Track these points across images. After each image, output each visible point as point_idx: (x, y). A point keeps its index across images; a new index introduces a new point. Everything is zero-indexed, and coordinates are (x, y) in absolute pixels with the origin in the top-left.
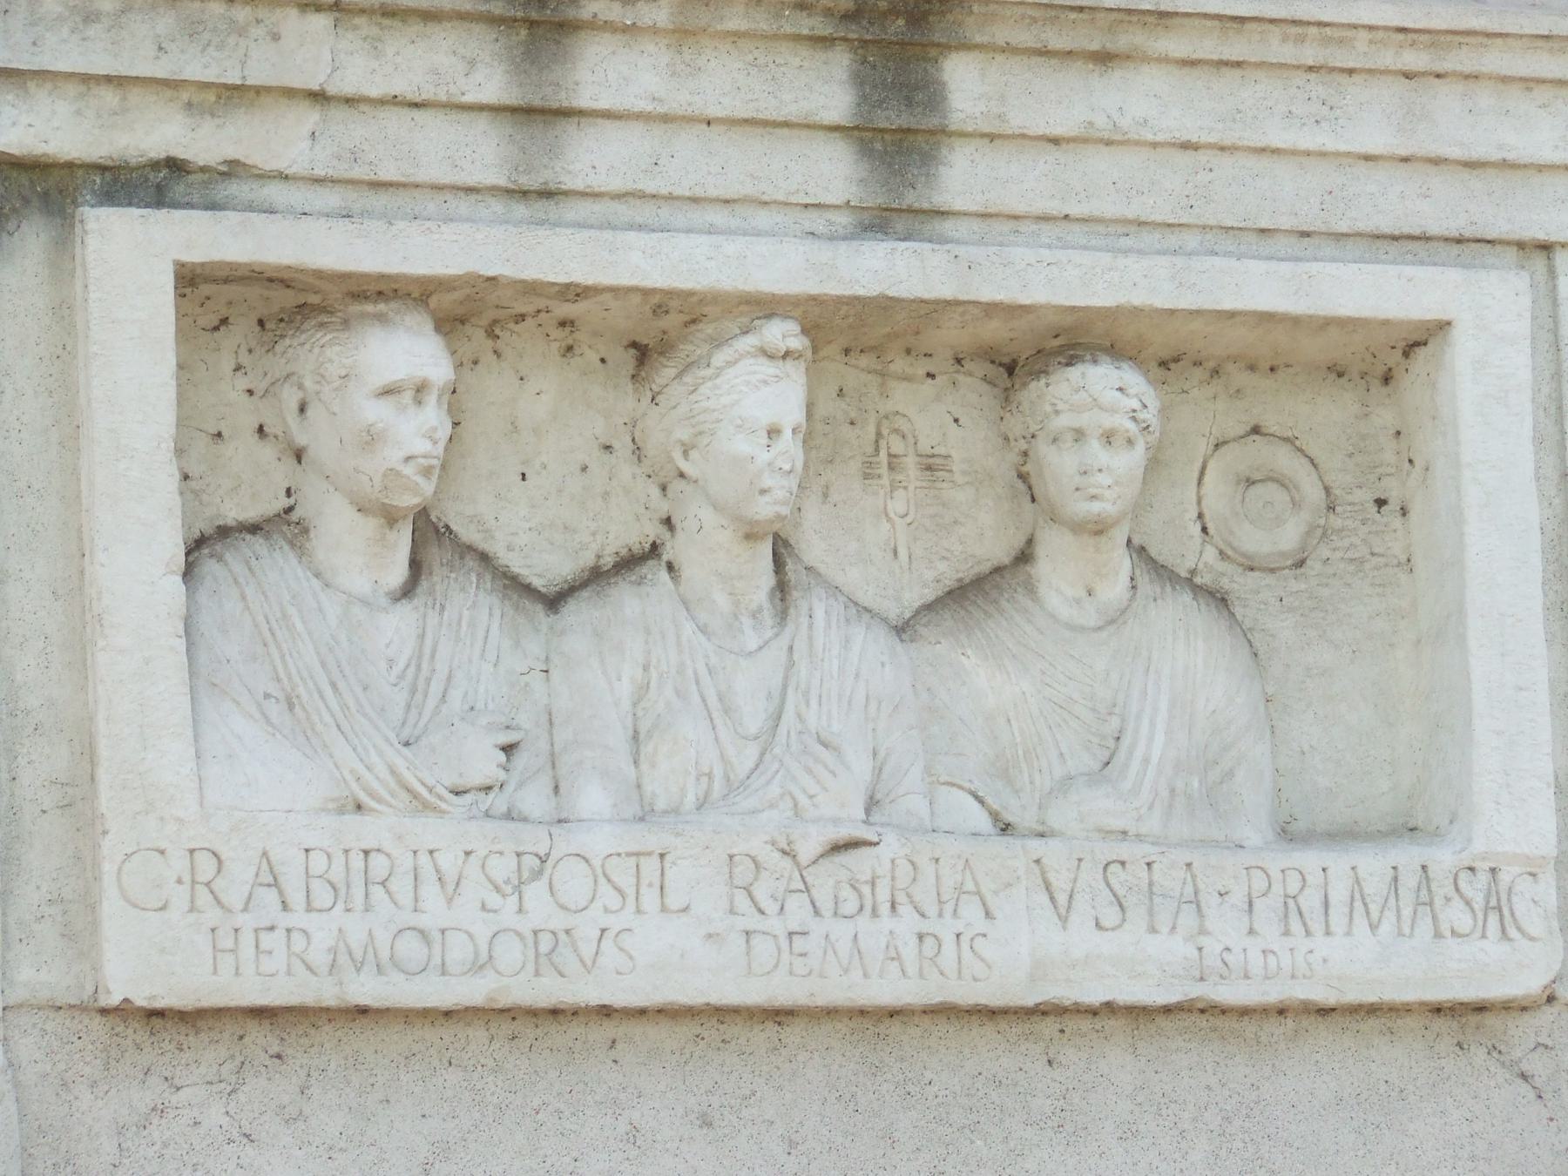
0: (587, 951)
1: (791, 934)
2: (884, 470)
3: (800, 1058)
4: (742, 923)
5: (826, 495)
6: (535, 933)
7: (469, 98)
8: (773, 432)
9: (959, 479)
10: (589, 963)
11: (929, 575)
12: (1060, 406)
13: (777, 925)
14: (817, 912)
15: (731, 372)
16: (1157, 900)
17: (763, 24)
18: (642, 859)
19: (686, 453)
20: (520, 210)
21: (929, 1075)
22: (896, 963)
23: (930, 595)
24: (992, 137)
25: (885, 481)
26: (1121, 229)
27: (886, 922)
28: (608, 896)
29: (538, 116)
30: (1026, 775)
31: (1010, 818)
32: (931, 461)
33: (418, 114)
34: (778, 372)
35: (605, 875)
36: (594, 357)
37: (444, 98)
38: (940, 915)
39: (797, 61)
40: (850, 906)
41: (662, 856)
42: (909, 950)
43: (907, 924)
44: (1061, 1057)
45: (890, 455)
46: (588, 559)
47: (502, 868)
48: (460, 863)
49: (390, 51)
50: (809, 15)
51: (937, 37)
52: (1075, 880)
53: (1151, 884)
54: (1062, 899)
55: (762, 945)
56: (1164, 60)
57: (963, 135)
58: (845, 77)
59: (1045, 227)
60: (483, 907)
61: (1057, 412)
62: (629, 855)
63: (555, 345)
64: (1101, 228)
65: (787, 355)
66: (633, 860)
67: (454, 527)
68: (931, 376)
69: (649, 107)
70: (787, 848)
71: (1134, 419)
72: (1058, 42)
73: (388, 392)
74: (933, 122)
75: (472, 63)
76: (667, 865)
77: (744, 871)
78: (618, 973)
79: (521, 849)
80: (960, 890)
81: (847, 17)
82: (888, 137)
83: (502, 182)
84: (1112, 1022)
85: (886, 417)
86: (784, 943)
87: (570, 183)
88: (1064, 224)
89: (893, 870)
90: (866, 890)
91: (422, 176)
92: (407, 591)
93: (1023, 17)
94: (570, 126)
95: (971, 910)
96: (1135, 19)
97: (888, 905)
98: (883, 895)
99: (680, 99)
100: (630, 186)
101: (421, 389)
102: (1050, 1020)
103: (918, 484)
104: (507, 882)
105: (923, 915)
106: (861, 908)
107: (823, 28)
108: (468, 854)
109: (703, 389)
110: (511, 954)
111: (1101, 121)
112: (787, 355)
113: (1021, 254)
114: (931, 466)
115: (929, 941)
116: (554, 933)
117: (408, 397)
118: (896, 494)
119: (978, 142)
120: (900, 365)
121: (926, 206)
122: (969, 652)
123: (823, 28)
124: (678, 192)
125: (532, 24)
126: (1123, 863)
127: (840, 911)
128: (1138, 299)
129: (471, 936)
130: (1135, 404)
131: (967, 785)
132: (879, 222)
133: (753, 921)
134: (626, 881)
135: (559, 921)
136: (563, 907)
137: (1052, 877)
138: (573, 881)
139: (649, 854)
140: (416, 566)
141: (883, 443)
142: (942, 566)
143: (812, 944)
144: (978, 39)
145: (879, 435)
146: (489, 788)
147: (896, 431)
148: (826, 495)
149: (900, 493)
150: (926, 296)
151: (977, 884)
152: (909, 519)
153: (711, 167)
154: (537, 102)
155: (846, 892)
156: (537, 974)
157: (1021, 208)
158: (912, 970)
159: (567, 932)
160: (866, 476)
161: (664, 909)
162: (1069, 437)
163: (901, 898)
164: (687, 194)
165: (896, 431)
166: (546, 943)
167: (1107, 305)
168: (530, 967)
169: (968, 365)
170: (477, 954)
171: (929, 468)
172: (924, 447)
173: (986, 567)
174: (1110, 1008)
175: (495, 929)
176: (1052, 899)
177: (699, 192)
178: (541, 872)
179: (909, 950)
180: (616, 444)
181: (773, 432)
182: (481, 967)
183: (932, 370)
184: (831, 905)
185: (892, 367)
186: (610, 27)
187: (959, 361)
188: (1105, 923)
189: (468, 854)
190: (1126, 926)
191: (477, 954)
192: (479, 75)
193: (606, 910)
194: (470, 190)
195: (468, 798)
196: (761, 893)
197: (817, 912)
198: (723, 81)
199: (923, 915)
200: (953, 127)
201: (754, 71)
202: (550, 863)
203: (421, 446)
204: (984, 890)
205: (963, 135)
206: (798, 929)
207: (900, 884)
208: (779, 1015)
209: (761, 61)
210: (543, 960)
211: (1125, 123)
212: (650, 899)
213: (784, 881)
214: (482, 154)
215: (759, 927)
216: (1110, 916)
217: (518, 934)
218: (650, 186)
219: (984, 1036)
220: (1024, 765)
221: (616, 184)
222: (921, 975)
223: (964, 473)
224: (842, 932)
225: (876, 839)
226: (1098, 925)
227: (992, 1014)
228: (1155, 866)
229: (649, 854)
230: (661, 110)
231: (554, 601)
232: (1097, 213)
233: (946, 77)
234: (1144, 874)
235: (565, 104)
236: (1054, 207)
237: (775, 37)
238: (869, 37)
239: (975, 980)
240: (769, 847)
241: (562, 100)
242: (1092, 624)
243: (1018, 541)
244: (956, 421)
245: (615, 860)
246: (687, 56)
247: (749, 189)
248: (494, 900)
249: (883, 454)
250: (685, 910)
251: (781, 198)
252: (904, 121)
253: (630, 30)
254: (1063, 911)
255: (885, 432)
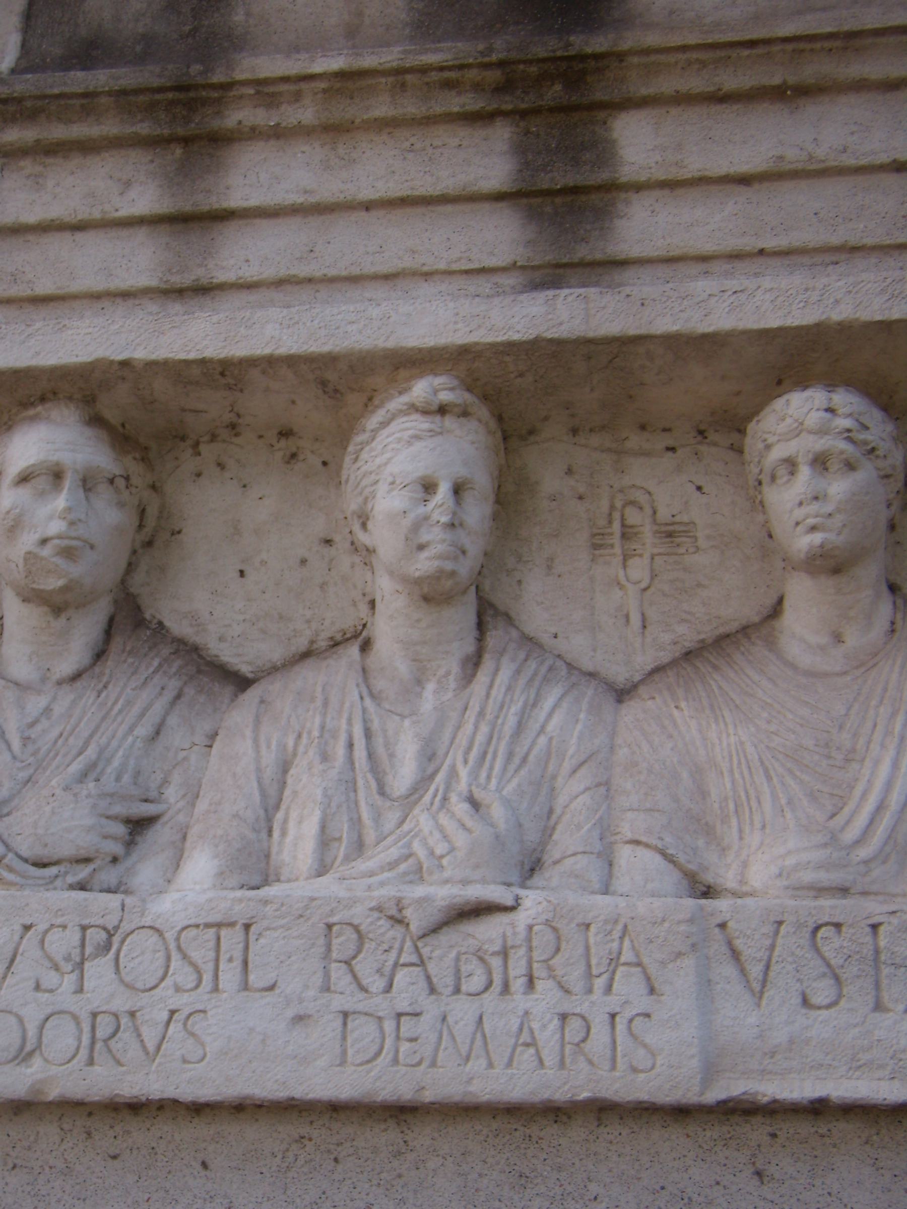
0: (150, 1037)
1: (399, 1015)
2: (616, 540)
3: (431, 1165)
4: (338, 1002)
5: (549, 568)
6: (94, 1015)
7: (123, 213)
8: (429, 487)
9: (701, 543)
10: (151, 1047)
11: (666, 638)
12: (771, 439)
13: (382, 1005)
14: (432, 990)
15: (385, 432)
16: (885, 971)
17: (411, 107)
18: (223, 932)
19: (364, 526)
20: (176, 307)
21: (594, 1188)
22: (532, 1051)
23: (665, 657)
24: (670, 185)
25: (618, 550)
26: (828, 258)
27: (520, 1001)
28: (181, 973)
29: (193, 222)
30: (735, 830)
31: (709, 878)
32: (671, 528)
33: (79, 236)
34: (432, 426)
35: (179, 948)
36: (316, 461)
37: (97, 215)
38: (590, 991)
39: (456, 142)
40: (476, 982)
41: (247, 927)
42: (547, 1035)
43: (545, 1000)
44: (772, 1169)
45: (623, 525)
46: (301, 644)
47: (63, 943)
48: (16, 937)
49: (50, 184)
50: (459, 94)
51: (599, 96)
52: (772, 947)
53: (877, 952)
54: (755, 971)
55: (363, 1032)
56: (860, 86)
57: (638, 187)
58: (505, 148)
59: (738, 264)
60: (38, 988)
61: (768, 447)
62: (208, 926)
63: (281, 453)
64: (806, 260)
65: (442, 410)
66: (212, 931)
67: (167, 623)
68: (672, 449)
69: (300, 199)
70: (398, 916)
71: (850, 440)
72: (730, 81)
73: (24, 479)
74: (603, 176)
75: (128, 184)
76: (252, 937)
77: (344, 942)
78: (185, 1061)
79: (86, 922)
80: (614, 961)
81: (499, 90)
82: (558, 200)
83: (154, 283)
84: (842, 1125)
85: (621, 491)
86: (389, 1026)
87: (221, 277)
88: (761, 260)
89: (529, 939)
90: (496, 963)
91: (76, 287)
92: (76, 677)
93: (689, 63)
94: (231, 229)
95: (628, 985)
96: (818, 45)
97: (523, 980)
98: (518, 968)
99: (331, 188)
100: (283, 273)
101: (57, 475)
102: (757, 1120)
103: (656, 551)
104: (68, 958)
105: (567, 992)
106: (489, 985)
107: (470, 102)
108: (27, 928)
109: (364, 455)
110: (62, 1039)
111: (791, 154)
112: (442, 410)
113: (703, 286)
114: (670, 533)
115: (575, 1024)
116: (116, 1016)
117: (42, 482)
118: (630, 562)
119: (657, 193)
120: (635, 440)
121: (598, 256)
122: (683, 704)
123: (470, 102)
124: (332, 272)
125: (186, 141)
126: (838, 926)
127: (464, 988)
128: (838, 314)
129: (21, 1021)
130: (847, 423)
131: (654, 841)
132: (549, 275)
133: (349, 1000)
134: (202, 954)
135: (122, 1003)
136: (129, 986)
137: (739, 943)
138: (141, 956)
139: (232, 924)
140: (99, 655)
141: (617, 516)
142: (681, 629)
143: (425, 1026)
144: (644, 91)
145: (612, 507)
146: (87, 860)
147: (632, 503)
148: (549, 568)
149: (632, 562)
150: (591, 334)
151: (637, 955)
152: (643, 585)
153: (373, 254)
154: (188, 208)
155: (471, 966)
156: (91, 1062)
157: (709, 247)
158: (550, 1059)
159: (132, 1014)
160: (596, 547)
161: (245, 986)
162: (782, 471)
163: (539, 970)
164: (344, 273)
165: (632, 503)
166: (104, 1027)
167: (804, 323)
168: (84, 1053)
169: (712, 436)
170: (24, 1039)
171: (670, 535)
172: (664, 514)
173: (734, 626)
174: (818, 1109)
175: (49, 1010)
176: (743, 971)
177: (355, 271)
178: (108, 946)
179: (547, 1035)
180: (337, 538)
181: (429, 487)
182: (31, 1054)
183: (671, 443)
184: (450, 980)
185: (628, 445)
186: (254, 134)
187: (701, 432)
188: (816, 1000)
189: (27, 928)
190: (843, 1003)
191: (24, 1039)
192: (133, 194)
193: (178, 989)
194: (126, 295)
195: (53, 870)
196: (365, 967)
197: (432, 990)
198: (379, 168)
199: (567, 992)
200: (623, 180)
201: (410, 156)
202: (116, 940)
203: (56, 527)
204: (646, 960)
205: (638, 187)
206: (408, 1009)
207: (536, 955)
208: (401, 1113)
209: (418, 146)
210: (99, 1045)
211: (820, 152)
212: (229, 976)
213: (393, 955)
214: (138, 261)
215: (360, 1007)
216: (822, 992)
217: (75, 1018)
218: (303, 270)
219: (669, 1141)
220: (734, 822)
221: (269, 273)
222: (562, 1064)
223: (709, 537)
224: (463, 1012)
225: (509, 902)
226: (805, 1002)
227: (681, 1113)
228: (882, 929)
229: (232, 924)
230: (312, 199)
231: (243, 683)
232: (796, 244)
233: (615, 135)
234: (869, 939)
235: (216, 206)
236: (750, 243)
237: (428, 121)
238: (523, 106)
239: (635, 1070)
240: (376, 914)
241: (217, 202)
242: (838, 669)
243: (770, 601)
244: (699, 488)
245: (193, 932)
246: (341, 150)
247: (407, 263)
248: (50, 979)
249: (616, 527)
250: (271, 988)
251: (442, 266)
252: (571, 179)
253: (278, 134)
254: (756, 986)
255: (619, 504)
